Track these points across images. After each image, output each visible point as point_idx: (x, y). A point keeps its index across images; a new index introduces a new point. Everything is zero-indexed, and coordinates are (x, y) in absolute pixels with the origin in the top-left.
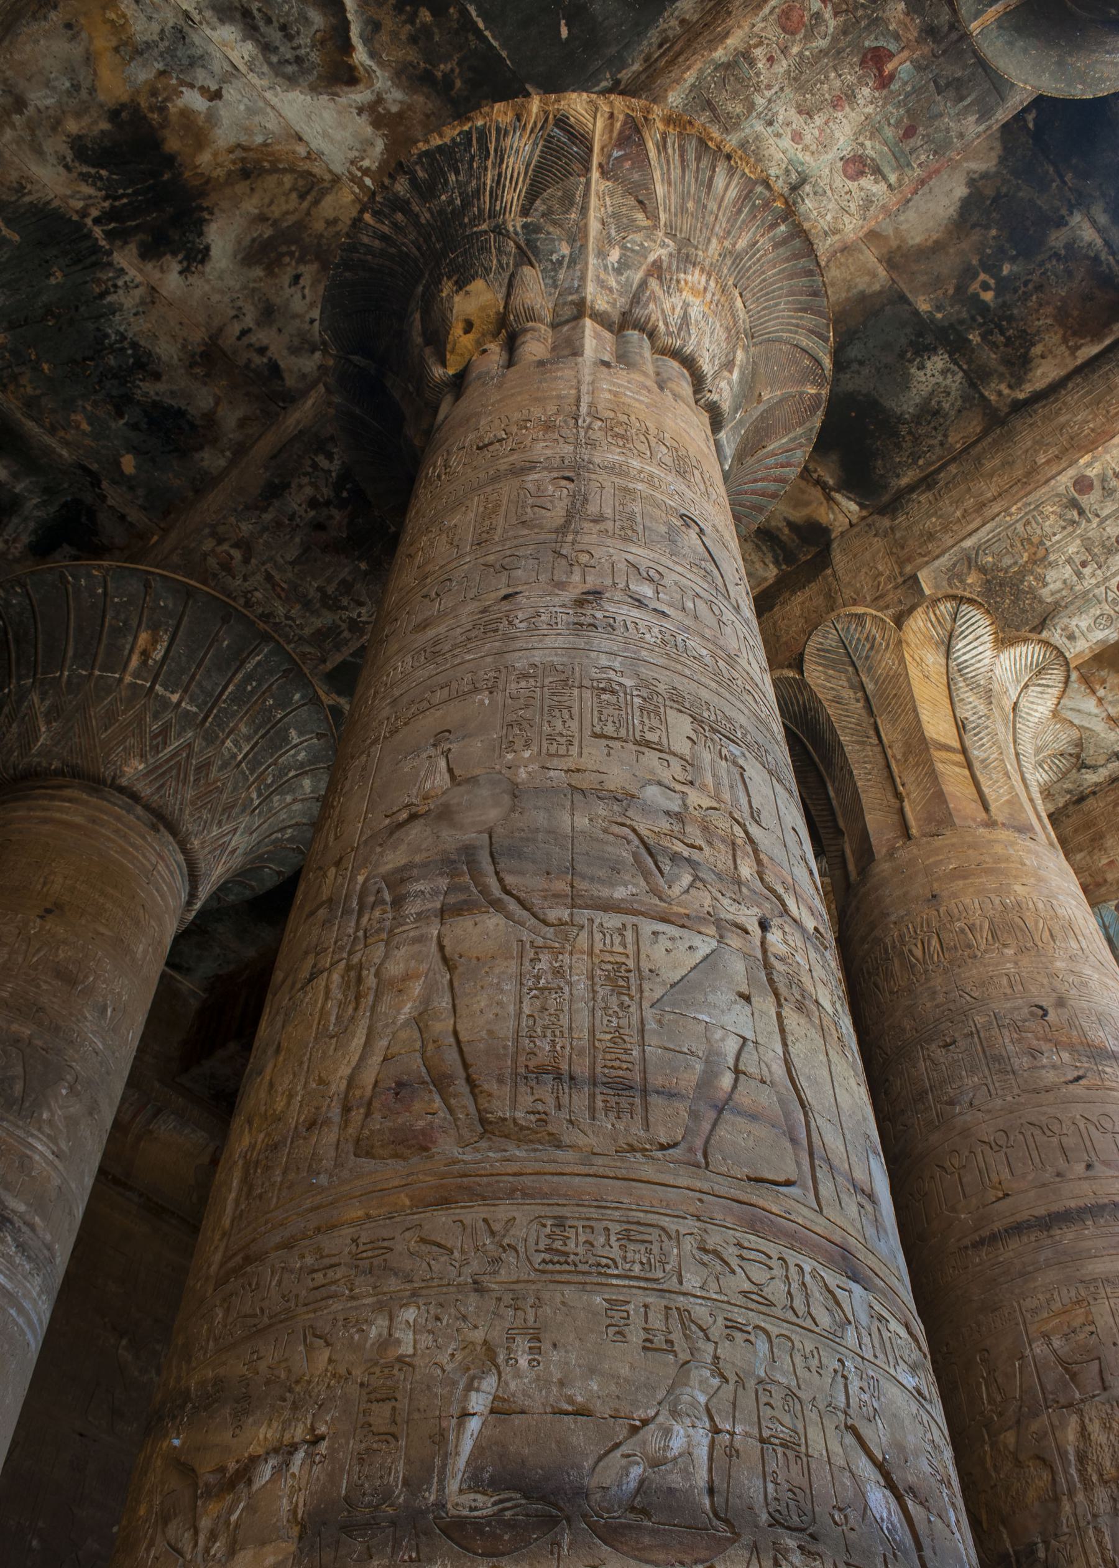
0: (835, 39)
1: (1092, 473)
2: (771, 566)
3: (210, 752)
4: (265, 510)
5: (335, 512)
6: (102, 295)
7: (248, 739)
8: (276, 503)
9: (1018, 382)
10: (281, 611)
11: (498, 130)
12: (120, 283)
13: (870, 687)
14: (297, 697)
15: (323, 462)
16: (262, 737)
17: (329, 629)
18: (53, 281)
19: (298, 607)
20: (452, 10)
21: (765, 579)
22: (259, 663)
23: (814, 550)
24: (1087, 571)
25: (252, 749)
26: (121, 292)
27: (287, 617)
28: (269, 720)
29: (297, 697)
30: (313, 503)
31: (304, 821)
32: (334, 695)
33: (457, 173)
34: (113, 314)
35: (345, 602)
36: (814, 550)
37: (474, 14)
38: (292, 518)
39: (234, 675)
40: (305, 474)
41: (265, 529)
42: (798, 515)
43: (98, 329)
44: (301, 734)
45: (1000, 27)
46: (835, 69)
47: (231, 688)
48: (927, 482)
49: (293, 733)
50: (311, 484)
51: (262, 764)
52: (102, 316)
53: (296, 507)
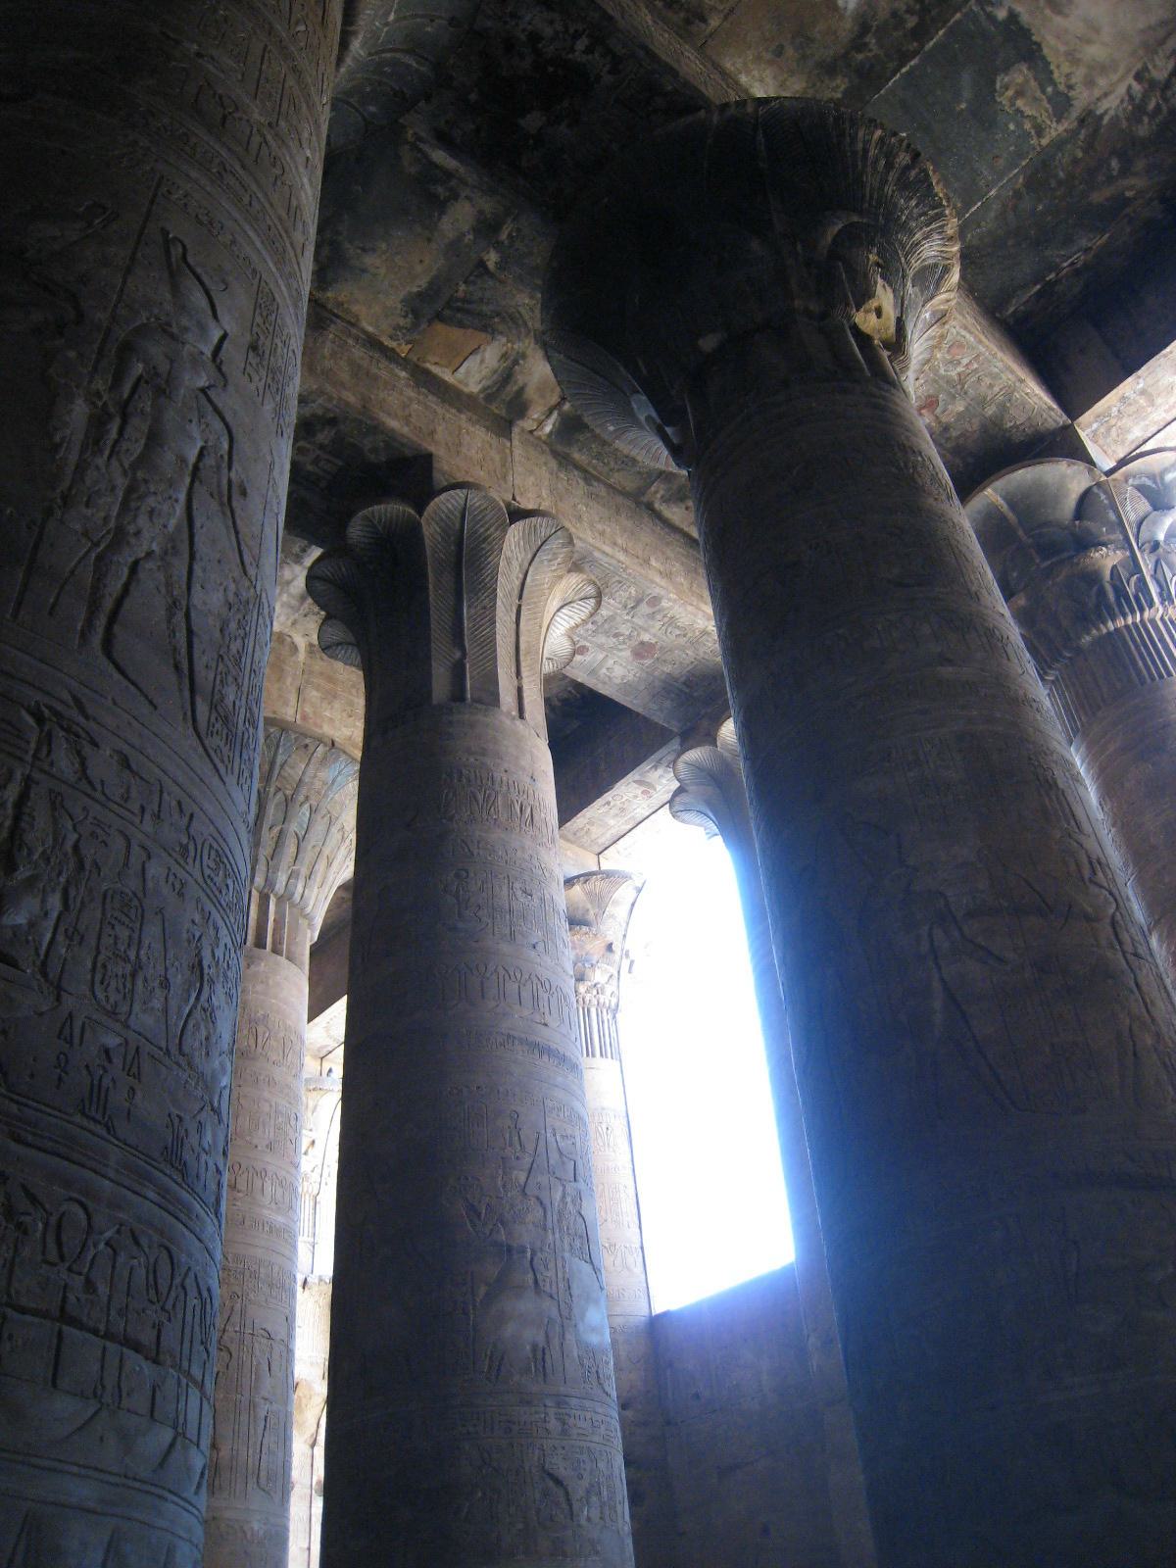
0: (943, 377)
1: (665, 604)
2: (480, 386)
9: (666, 500)
11: (942, 226)
13: (528, 579)
14: (372, 109)
15: (581, 44)
20: (915, 44)
21: (467, 385)
22: (408, 66)
23: (503, 413)
24: (590, 626)
29: (372, 109)
30: (535, 37)
33: (917, 206)
36: (503, 413)
37: (912, 63)
38: (513, 16)
42: (530, 393)
45: (989, 504)
46: (926, 381)
48: (588, 477)
50: (557, 33)
53: (528, 18)
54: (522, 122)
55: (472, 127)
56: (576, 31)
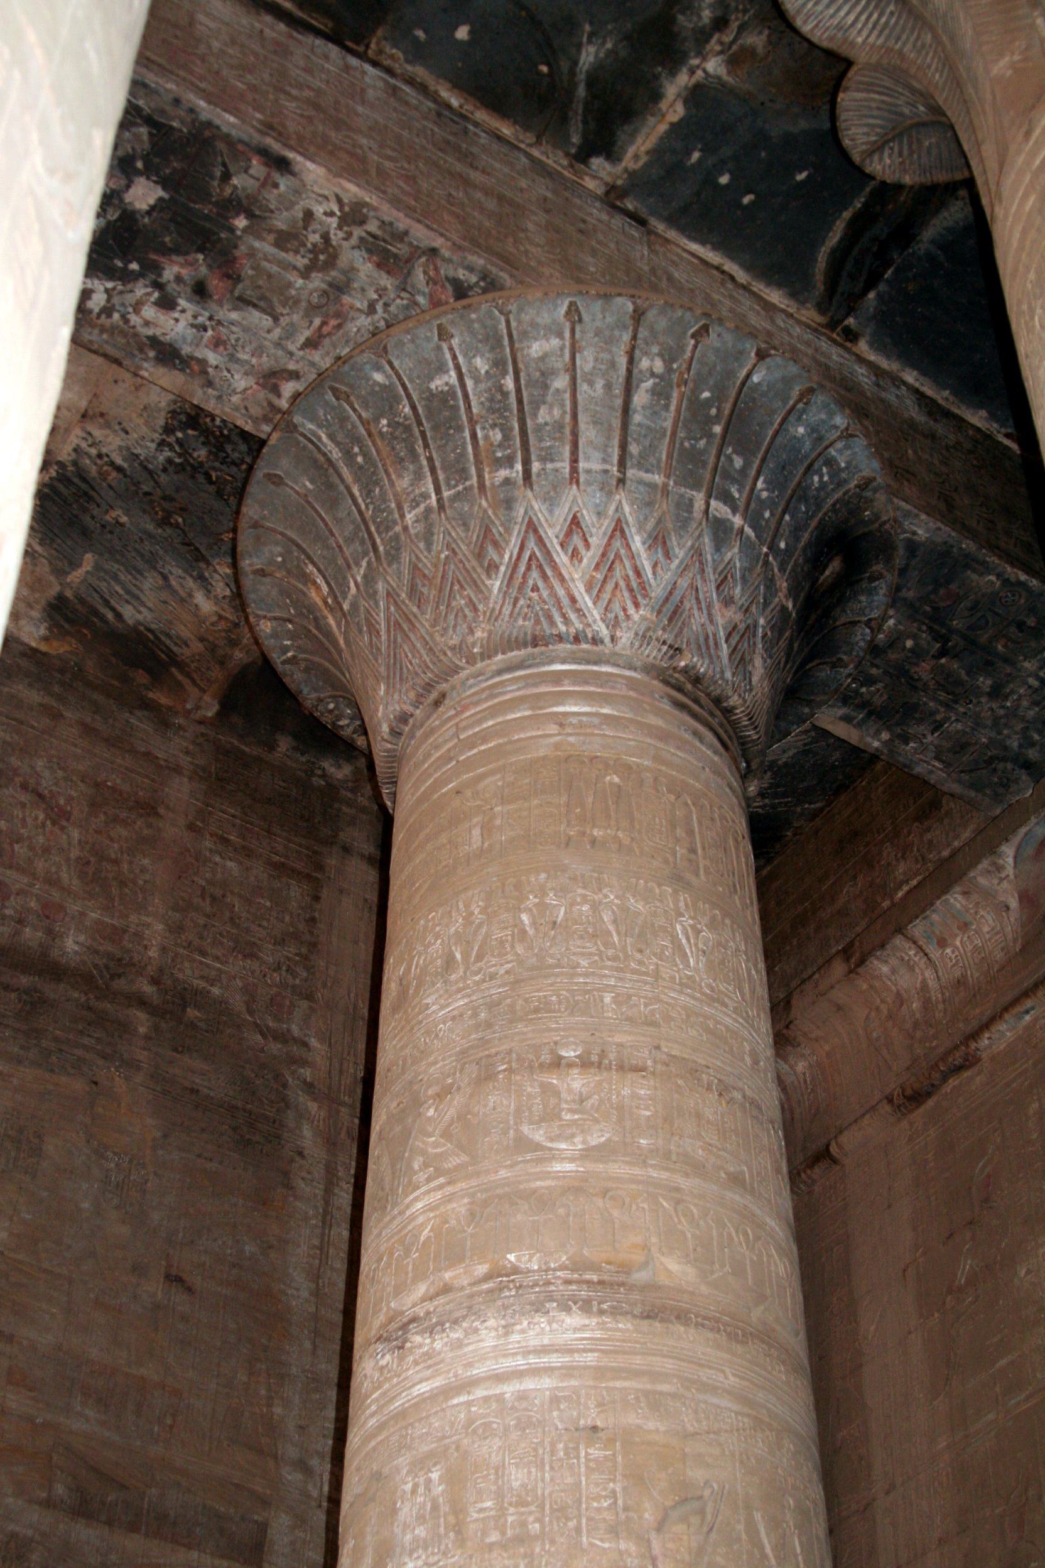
3: (405, 557)
4: (203, 362)
5: (169, 273)
6: (119, 469)
7: (418, 476)
8: (186, 350)
10: (364, 321)
12: (93, 451)
14: (378, 377)
16: (426, 446)
17: (370, 251)
18: (124, 519)
19: (346, 299)
22: (331, 437)
25: (433, 470)
26: (104, 450)
27: (371, 309)
28: (408, 429)
29: (378, 377)
30: (167, 303)
31: (626, 337)
32: (663, 105)
34: (137, 456)
35: (315, 238)
39: (342, 480)
40: (127, 321)
41: (232, 358)
43: (165, 470)
44: (441, 369)
47: (356, 491)
49: (437, 384)
50: (137, 311)
51: (463, 454)
52: (146, 468)
54: (160, 193)
55: (235, 181)
56: (109, 316)
